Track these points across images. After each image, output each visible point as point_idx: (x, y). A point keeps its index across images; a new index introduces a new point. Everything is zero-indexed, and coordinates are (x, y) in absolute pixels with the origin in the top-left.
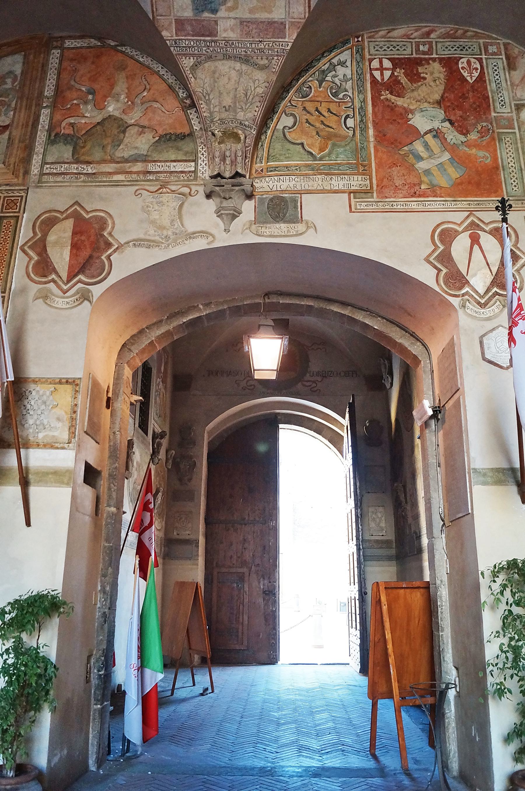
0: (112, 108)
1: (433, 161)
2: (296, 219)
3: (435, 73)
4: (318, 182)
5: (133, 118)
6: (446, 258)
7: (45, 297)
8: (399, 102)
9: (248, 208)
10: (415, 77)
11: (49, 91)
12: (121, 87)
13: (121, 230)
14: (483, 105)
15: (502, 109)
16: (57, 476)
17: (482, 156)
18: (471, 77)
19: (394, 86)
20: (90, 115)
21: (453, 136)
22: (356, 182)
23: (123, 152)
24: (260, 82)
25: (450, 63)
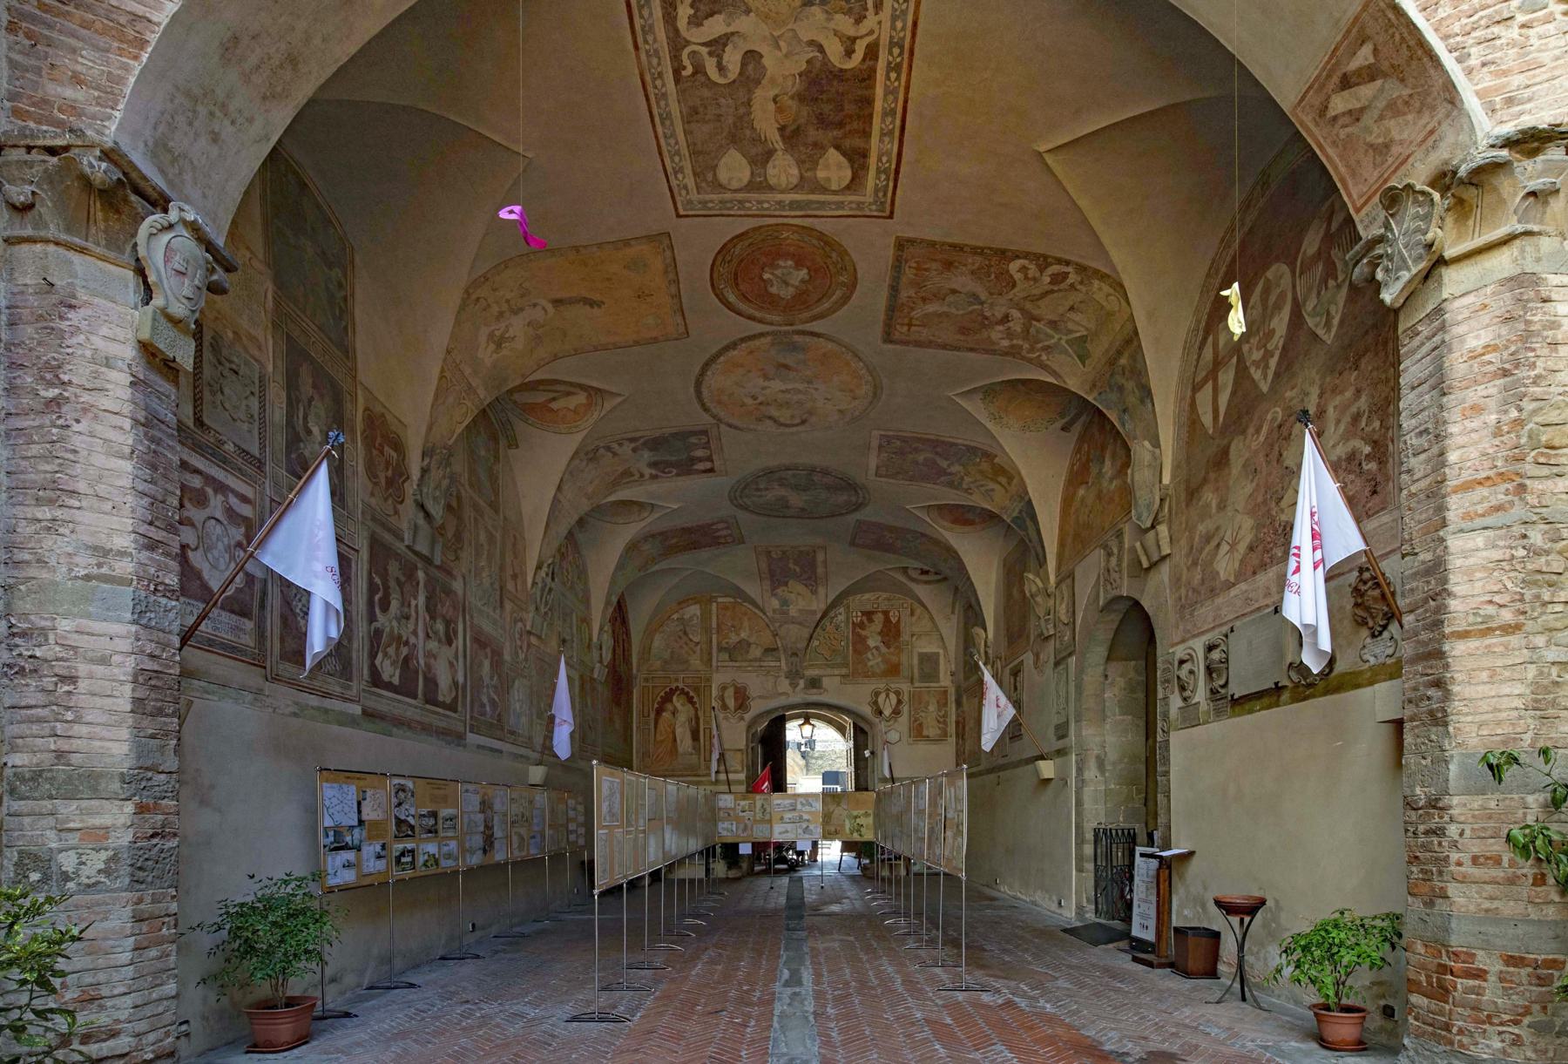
0: (743, 635)
1: (874, 661)
2: (820, 687)
3: (879, 619)
4: (829, 671)
5: (752, 640)
6: (876, 703)
7: (726, 718)
8: (863, 633)
9: (802, 682)
10: (871, 620)
11: (714, 625)
12: (746, 624)
13: (753, 691)
14: (898, 634)
15: (905, 637)
16: (739, 782)
17: (894, 659)
18: (894, 620)
19: (862, 625)
20: (734, 638)
21: (884, 649)
22: (844, 671)
23: (750, 657)
24: (806, 633)
25: (886, 613)
